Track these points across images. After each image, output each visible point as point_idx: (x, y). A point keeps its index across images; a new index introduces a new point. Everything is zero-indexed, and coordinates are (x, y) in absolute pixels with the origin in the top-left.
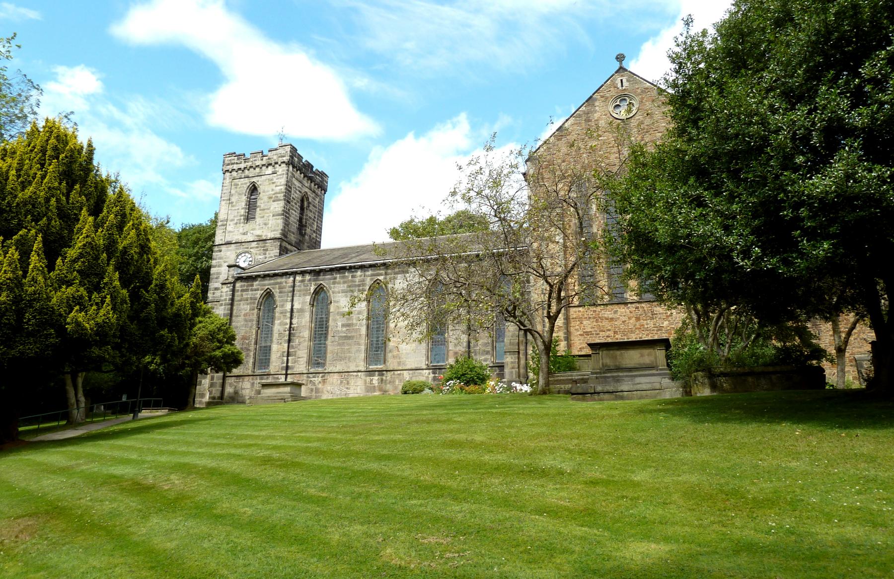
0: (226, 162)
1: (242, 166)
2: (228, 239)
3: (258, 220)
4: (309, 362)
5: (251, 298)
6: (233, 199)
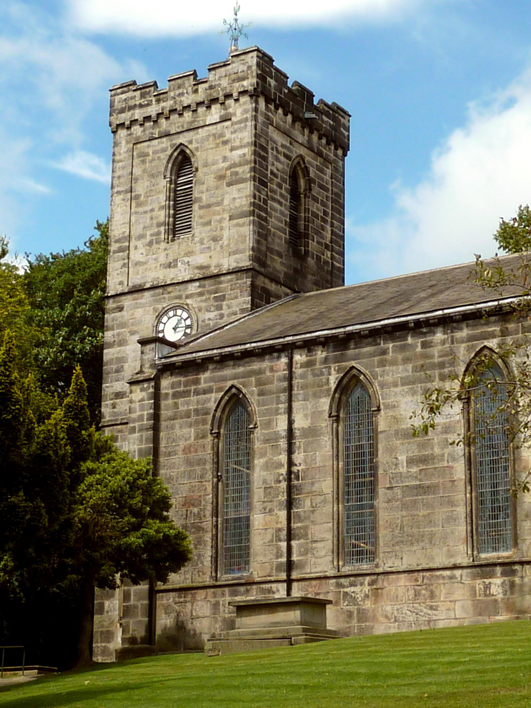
0: (118, 105)
1: (153, 110)
2: (136, 280)
3: (199, 231)
4: (340, 550)
5: (196, 411)
6: (140, 188)
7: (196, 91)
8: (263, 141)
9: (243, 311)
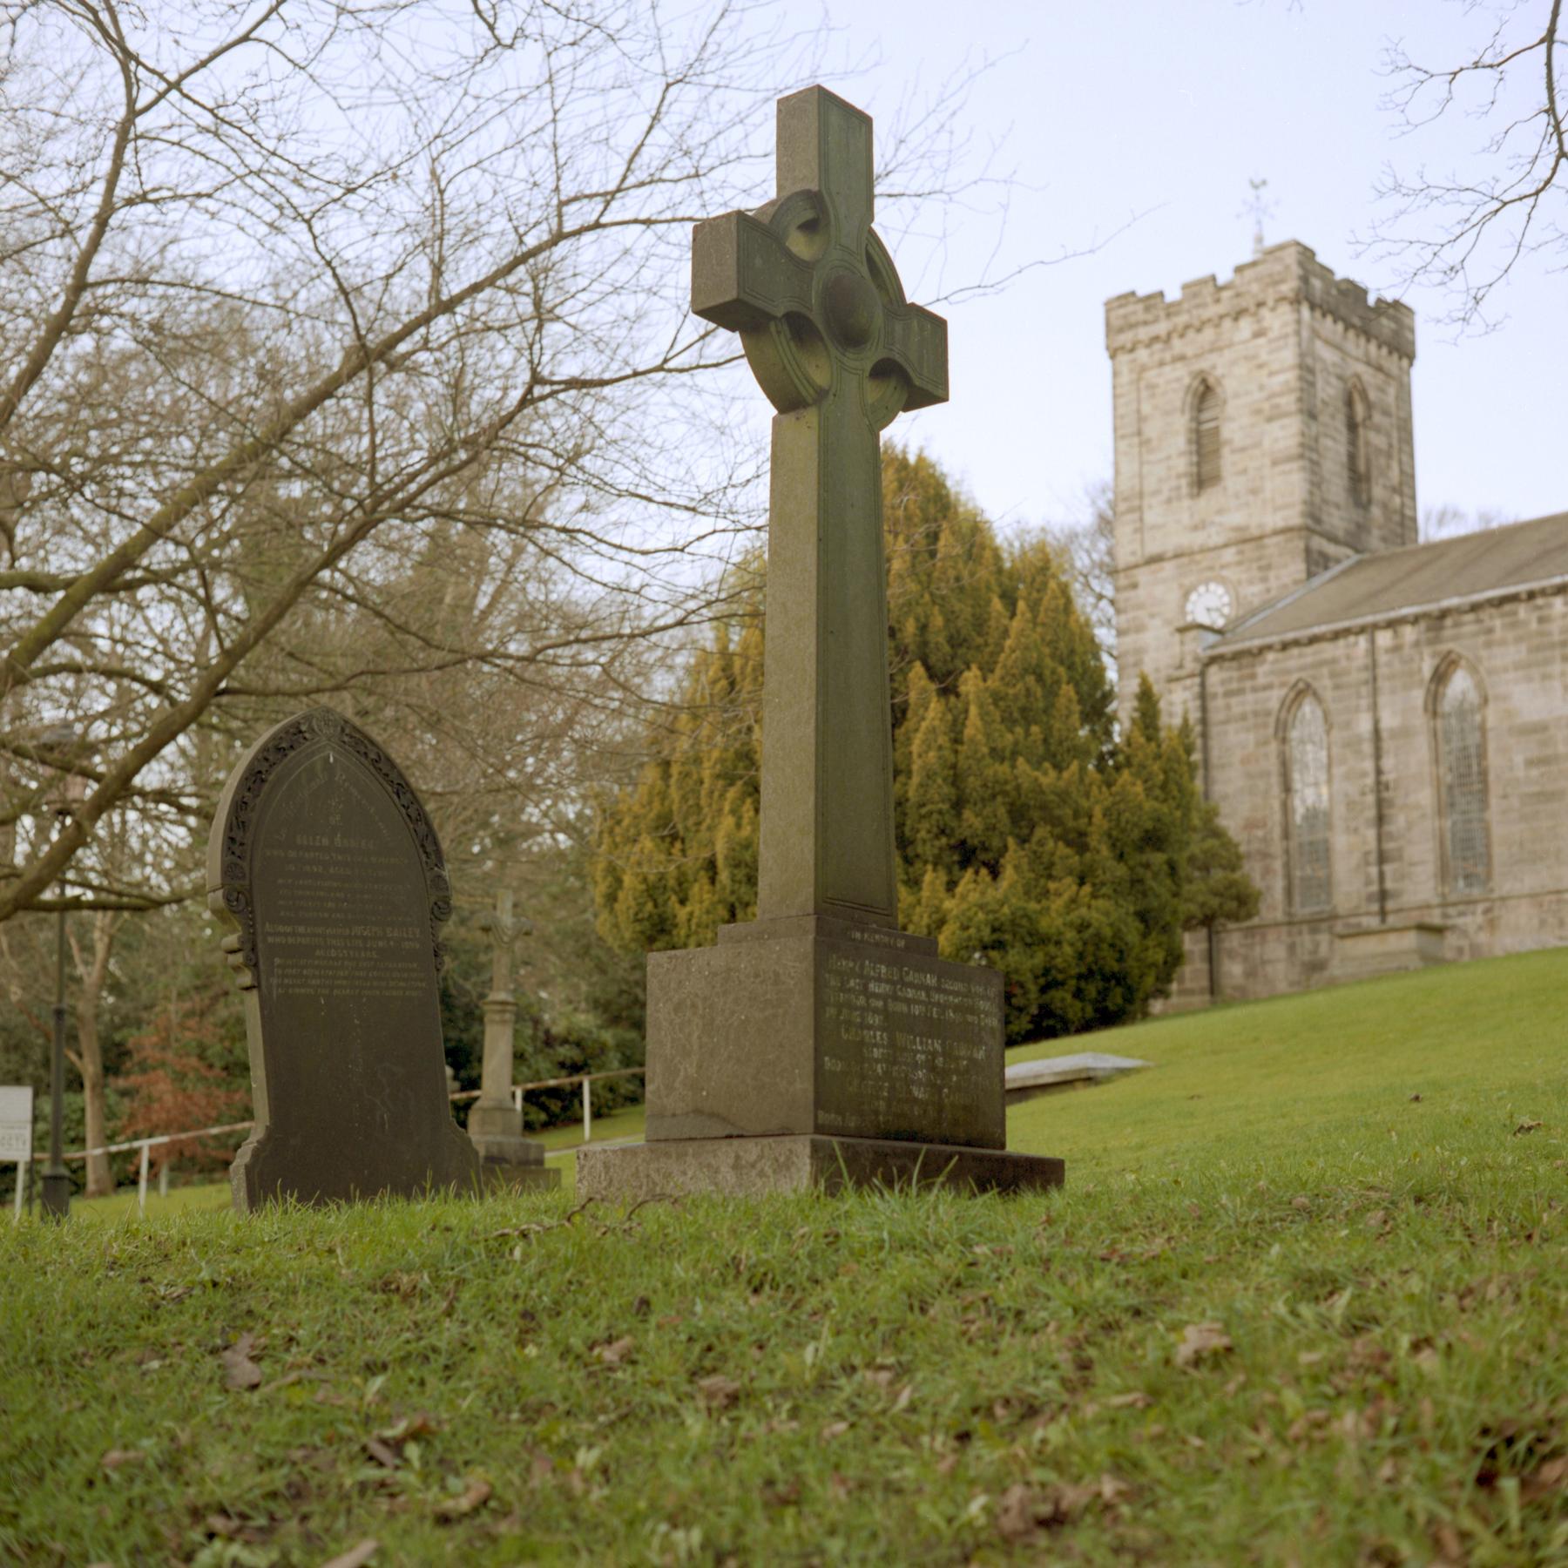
0: (1116, 323)
1: (1162, 328)
2: (1153, 548)
3: (1232, 482)
4: (1444, 873)
5: (1256, 714)
6: (1151, 430)
7: (1218, 301)
8: (1309, 361)
9: (1296, 582)
